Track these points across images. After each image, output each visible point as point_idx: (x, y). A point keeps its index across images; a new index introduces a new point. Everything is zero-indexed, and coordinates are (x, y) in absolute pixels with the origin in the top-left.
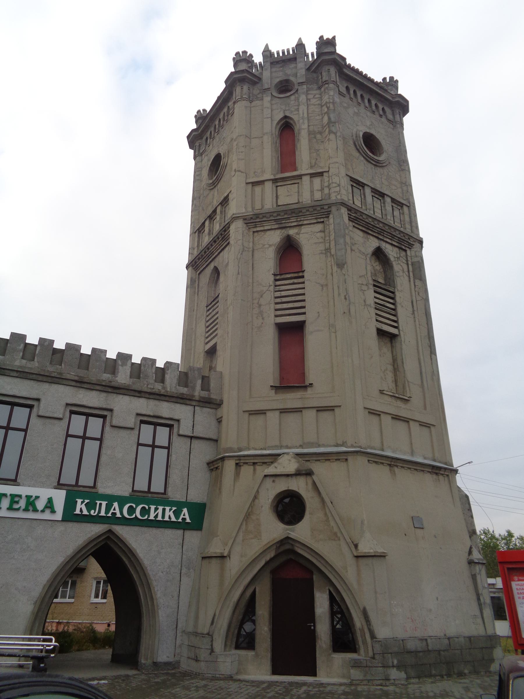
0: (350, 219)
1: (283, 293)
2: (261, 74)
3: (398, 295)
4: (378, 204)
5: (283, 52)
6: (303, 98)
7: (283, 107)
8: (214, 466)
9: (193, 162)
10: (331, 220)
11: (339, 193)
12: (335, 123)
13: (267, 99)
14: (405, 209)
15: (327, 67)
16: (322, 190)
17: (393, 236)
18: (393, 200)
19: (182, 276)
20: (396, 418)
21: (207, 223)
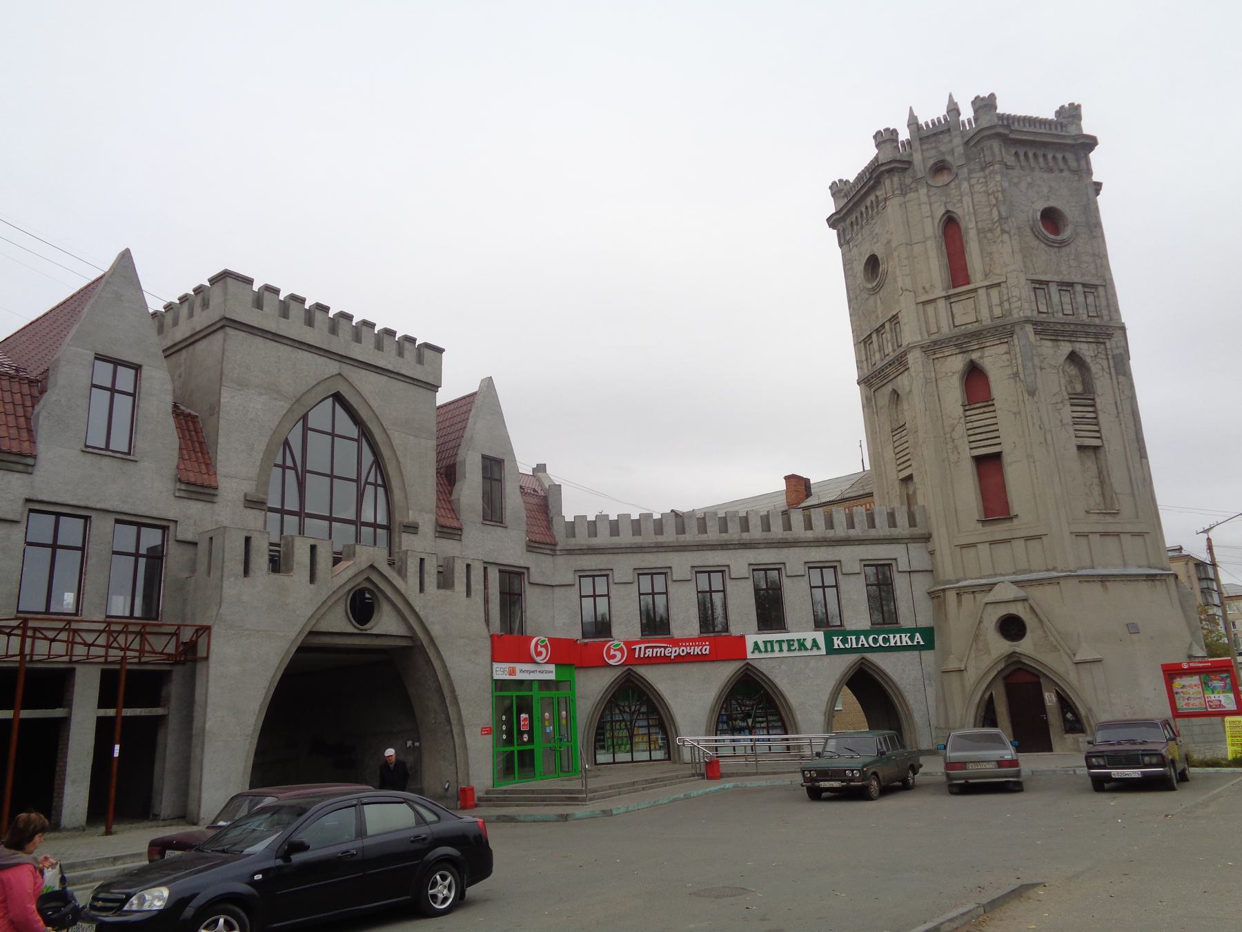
0: (1036, 333)
1: (976, 424)
2: (911, 155)
3: (1098, 400)
4: (1066, 299)
5: (933, 123)
6: (965, 185)
7: (944, 199)
8: (936, 596)
9: (838, 252)
10: (1016, 341)
11: (1021, 308)
12: (1007, 218)
13: (923, 191)
14: (1101, 290)
15: (987, 143)
16: (1001, 304)
17: (1087, 333)
18: (1084, 285)
19: (854, 395)
20: (1105, 534)
21: (874, 336)
